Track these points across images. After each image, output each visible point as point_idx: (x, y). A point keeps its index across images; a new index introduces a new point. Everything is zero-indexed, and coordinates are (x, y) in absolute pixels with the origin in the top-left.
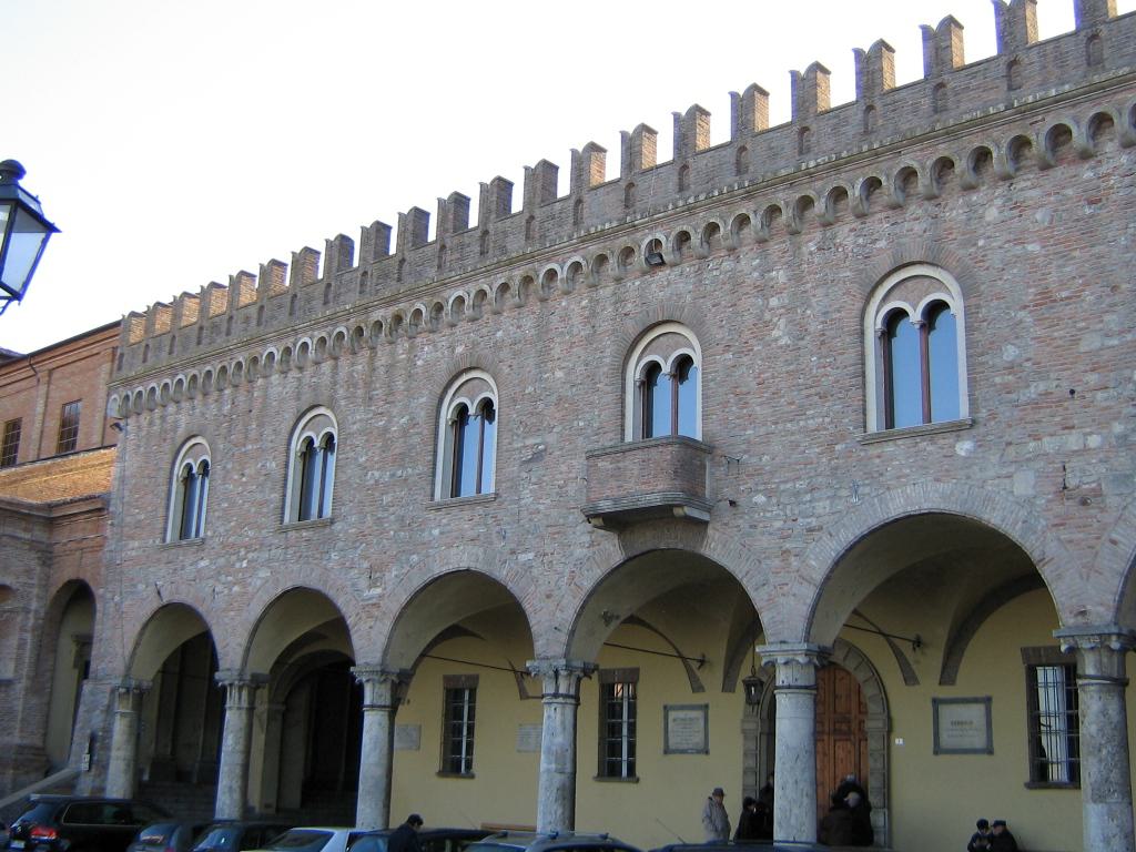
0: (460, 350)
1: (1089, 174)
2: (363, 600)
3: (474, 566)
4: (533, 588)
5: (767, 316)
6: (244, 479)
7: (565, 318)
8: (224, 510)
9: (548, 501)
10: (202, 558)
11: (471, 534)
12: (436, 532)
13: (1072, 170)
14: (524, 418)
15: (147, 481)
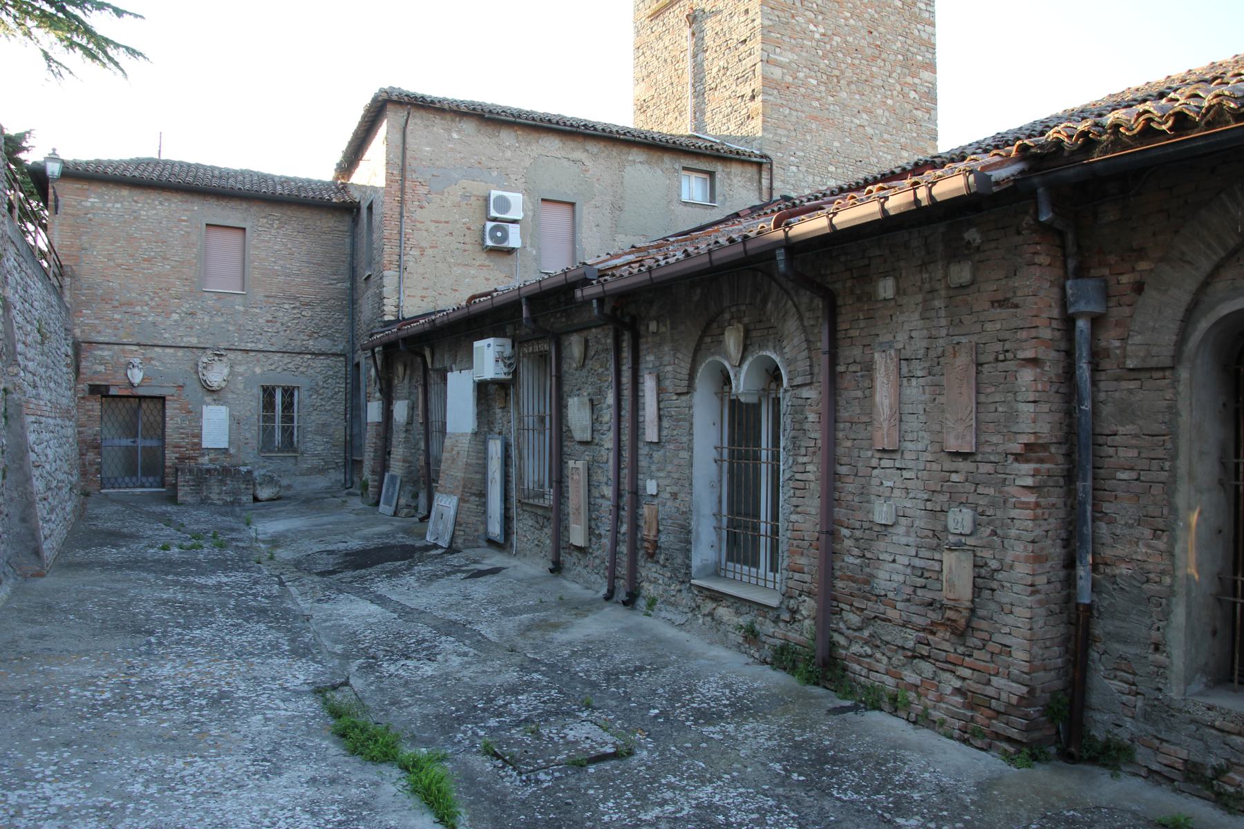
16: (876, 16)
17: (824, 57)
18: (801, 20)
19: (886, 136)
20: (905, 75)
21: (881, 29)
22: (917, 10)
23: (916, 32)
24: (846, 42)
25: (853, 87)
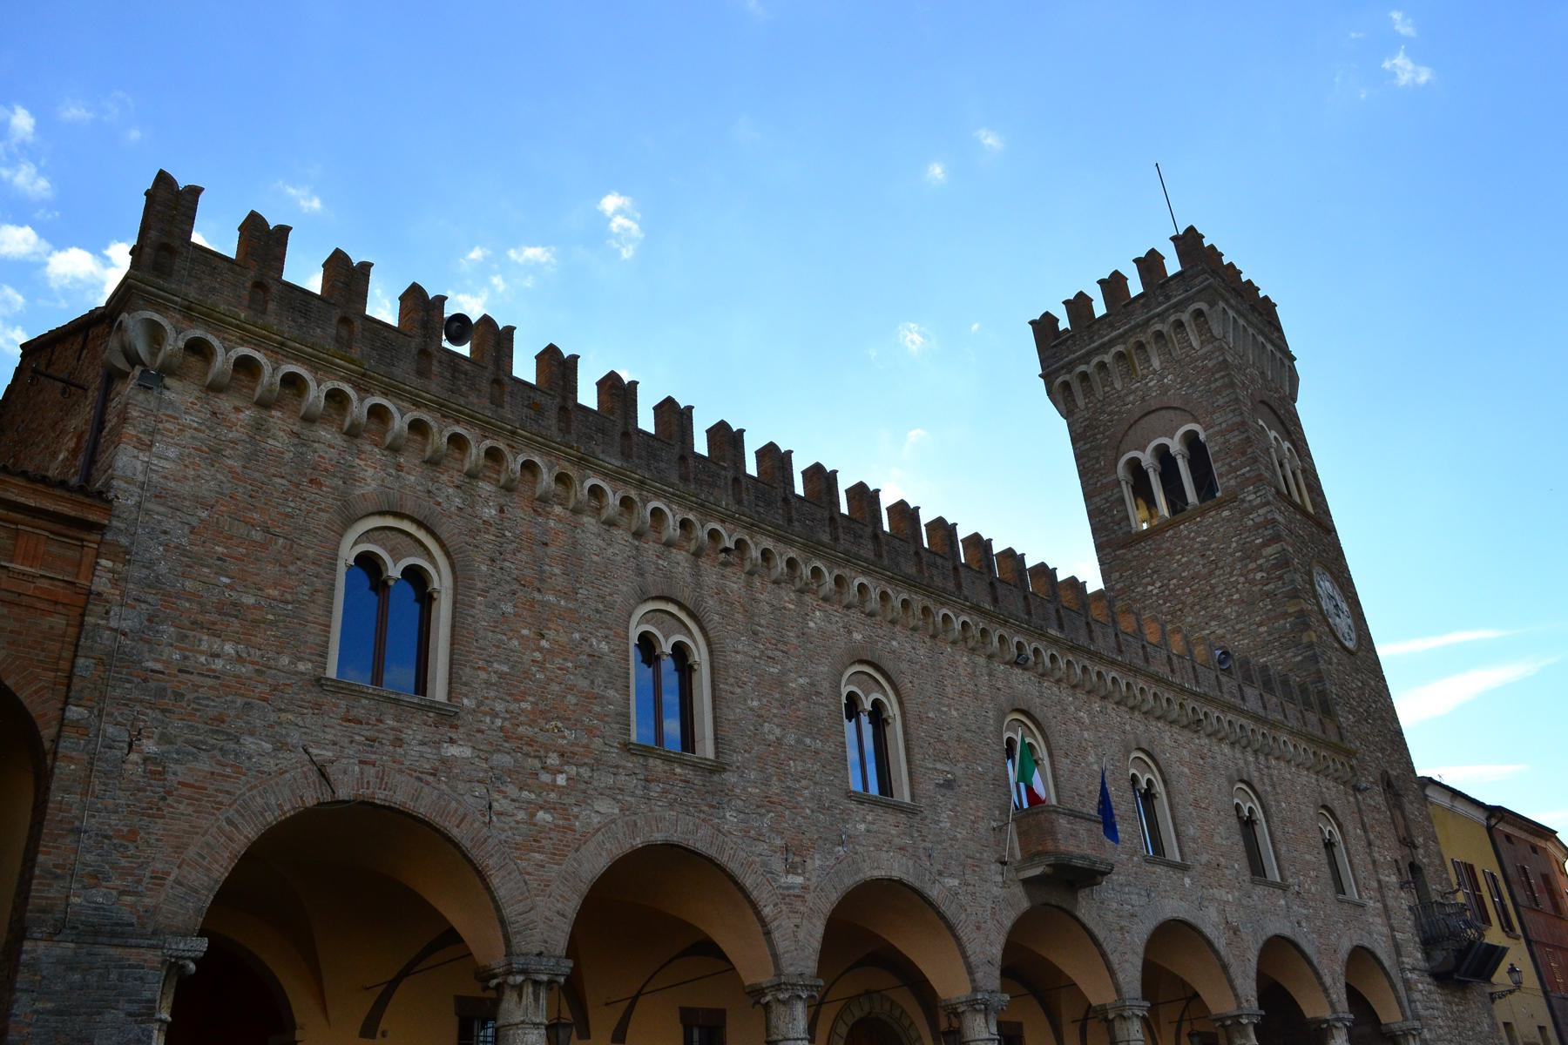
0: (857, 636)
1: (1197, 741)
2: (780, 887)
3: (905, 878)
4: (963, 916)
5: (1084, 744)
6: (544, 643)
7: (952, 663)
8: (502, 675)
9: (964, 832)
10: (452, 741)
11: (897, 841)
12: (862, 827)
13: (1191, 735)
14: (932, 741)
15: (257, 535)
16: (1206, 539)
17: (1165, 603)
18: (1139, 589)
19: (1237, 627)
20: (1246, 565)
21: (1213, 546)
22: (1246, 505)
23: (1251, 522)
24: (1181, 578)
25: (1197, 607)
